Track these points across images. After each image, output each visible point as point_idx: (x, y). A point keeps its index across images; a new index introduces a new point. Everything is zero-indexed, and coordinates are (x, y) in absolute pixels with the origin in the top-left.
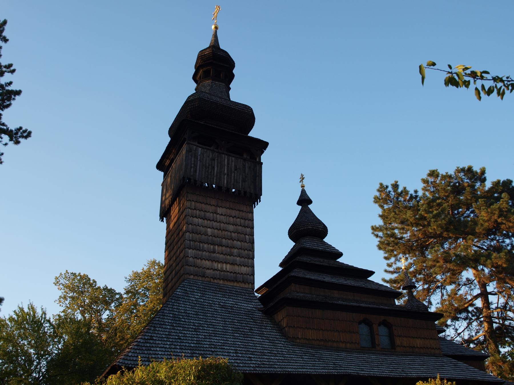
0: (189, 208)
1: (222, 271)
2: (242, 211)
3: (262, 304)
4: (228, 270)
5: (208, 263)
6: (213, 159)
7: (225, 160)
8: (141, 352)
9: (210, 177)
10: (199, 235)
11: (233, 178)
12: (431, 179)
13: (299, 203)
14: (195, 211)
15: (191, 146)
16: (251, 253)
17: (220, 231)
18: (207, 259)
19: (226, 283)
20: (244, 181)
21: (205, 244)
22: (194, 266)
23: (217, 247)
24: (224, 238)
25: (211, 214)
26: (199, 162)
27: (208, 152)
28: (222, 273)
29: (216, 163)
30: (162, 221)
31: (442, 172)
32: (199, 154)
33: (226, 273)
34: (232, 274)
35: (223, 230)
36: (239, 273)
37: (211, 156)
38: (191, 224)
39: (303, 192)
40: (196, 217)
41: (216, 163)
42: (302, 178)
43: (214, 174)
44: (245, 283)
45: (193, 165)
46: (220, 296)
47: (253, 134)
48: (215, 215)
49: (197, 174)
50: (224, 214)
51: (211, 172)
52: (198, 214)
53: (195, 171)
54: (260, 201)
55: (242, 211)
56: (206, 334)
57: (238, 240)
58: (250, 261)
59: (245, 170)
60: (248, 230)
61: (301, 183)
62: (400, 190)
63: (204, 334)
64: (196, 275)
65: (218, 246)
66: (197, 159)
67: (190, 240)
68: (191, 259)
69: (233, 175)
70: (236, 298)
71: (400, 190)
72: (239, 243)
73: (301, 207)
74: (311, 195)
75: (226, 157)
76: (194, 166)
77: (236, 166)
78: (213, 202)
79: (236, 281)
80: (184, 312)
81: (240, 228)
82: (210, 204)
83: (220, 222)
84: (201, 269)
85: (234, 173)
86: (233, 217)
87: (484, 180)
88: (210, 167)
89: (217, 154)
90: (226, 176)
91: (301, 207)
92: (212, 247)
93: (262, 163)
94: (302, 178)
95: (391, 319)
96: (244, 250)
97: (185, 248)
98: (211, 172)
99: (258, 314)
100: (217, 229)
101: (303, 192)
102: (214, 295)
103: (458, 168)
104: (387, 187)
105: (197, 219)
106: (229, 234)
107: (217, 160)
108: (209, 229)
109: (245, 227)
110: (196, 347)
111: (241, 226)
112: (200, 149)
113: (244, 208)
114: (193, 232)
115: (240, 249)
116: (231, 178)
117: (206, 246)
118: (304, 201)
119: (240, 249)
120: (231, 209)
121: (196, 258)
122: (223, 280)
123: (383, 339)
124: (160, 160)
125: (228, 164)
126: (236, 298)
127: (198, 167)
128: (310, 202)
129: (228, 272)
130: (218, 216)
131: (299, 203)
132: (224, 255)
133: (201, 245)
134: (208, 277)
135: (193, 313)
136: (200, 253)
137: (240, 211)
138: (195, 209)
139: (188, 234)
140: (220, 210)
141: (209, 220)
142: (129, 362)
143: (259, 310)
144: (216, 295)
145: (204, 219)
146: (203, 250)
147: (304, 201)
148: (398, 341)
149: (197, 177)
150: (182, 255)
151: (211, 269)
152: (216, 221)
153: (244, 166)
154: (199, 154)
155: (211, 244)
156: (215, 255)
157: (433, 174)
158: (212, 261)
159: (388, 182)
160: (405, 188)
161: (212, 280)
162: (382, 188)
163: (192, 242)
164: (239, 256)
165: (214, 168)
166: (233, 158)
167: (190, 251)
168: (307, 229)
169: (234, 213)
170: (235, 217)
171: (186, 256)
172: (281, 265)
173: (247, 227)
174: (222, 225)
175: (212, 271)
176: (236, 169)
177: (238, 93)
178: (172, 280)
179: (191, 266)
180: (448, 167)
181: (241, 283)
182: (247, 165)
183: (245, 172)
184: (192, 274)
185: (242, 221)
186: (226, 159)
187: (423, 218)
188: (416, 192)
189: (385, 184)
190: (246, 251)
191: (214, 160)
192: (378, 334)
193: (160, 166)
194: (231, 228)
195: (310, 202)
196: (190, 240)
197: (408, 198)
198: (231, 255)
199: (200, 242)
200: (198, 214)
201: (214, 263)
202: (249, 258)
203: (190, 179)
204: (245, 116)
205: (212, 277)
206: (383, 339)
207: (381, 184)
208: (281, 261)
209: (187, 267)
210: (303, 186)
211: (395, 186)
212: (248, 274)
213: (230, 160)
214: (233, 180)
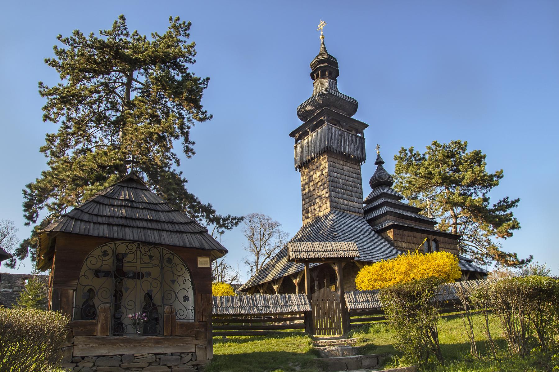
13: (376, 164)
19: (351, 213)
20: (357, 150)
30: (296, 170)
39: (379, 156)
53: (333, 143)
54: (364, 163)
62: (413, 153)
71: (413, 153)
74: (383, 158)
78: (341, 162)
87: (464, 150)
95: (438, 238)
101: (379, 156)
104: (406, 150)
118: (379, 162)
128: (383, 163)
131: (376, 164)
140: (344, 167)
145: (338, 173)
146: (339, 193)
147: (379, 162)
156: (344, 196)
162: (403, 150)
168: (381, 181)
169: (352, 170)
176: (352, 142)
177: (343, 87)
187: (430, 173)
188: (424, 155)
193: (292, 134)
194: (351, 179)
203: (330, 148)
207: (403, 148)
211: (411, 150)
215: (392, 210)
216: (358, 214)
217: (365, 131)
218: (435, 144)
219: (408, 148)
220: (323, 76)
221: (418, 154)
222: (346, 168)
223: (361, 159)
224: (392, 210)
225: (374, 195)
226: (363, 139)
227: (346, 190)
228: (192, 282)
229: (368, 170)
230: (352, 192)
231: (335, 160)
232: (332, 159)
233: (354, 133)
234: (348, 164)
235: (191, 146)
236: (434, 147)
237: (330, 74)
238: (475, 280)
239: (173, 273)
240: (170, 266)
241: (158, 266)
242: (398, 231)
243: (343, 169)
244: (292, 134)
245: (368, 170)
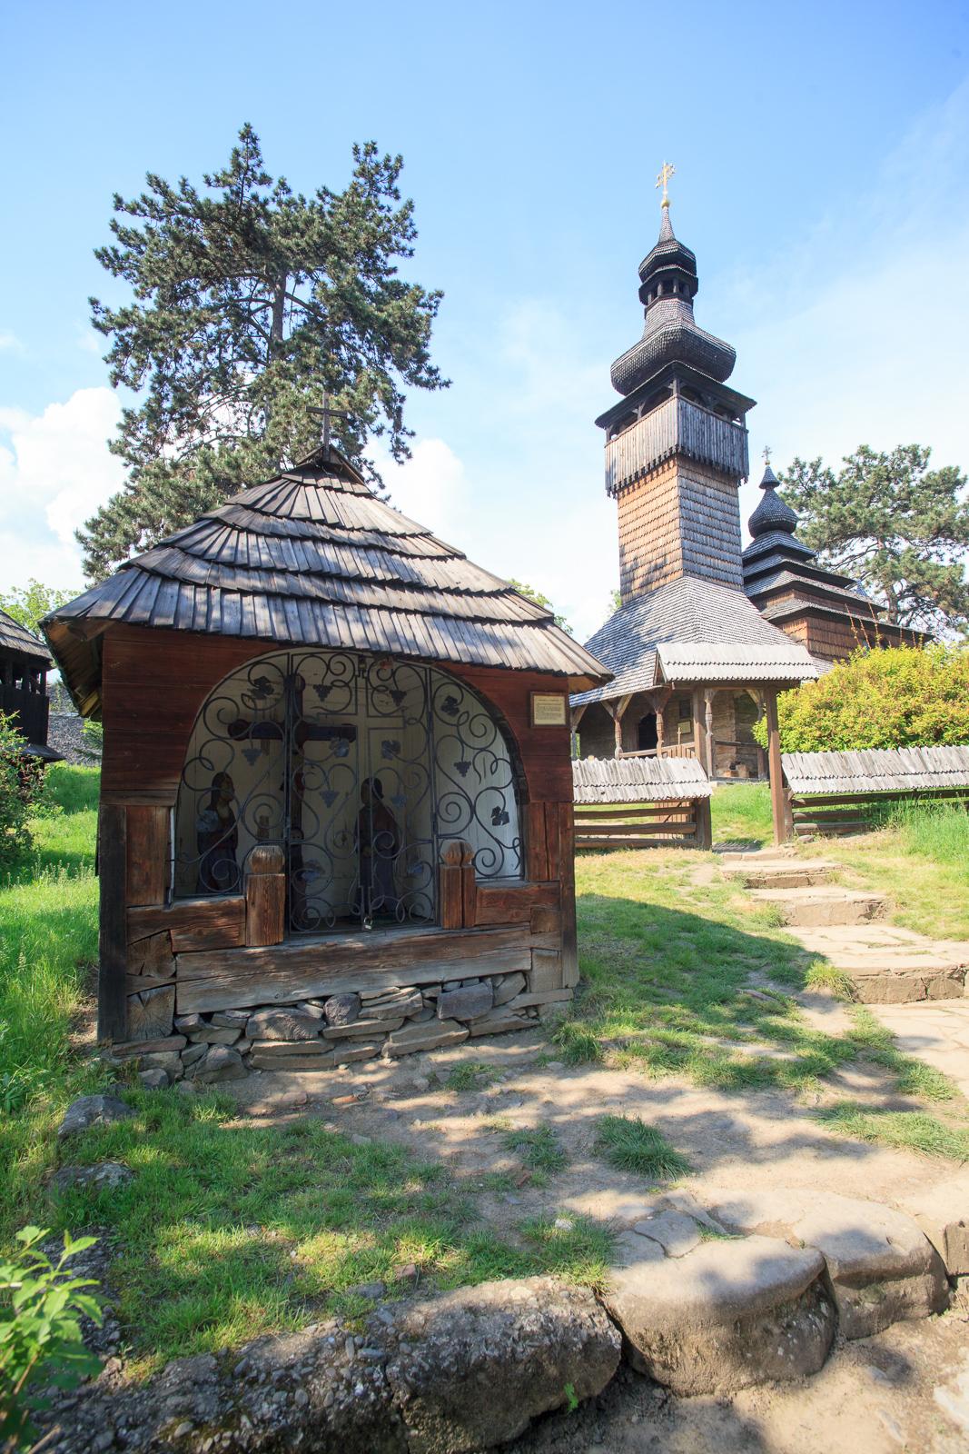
5: (701, 558)
13: (763, 486)
20: (733, 455)
31: (875, 449)
39: (768, 471)
62: (820, 471)
78: (702, 479)
101: (768, 471)
131: (763, 486)
140: (709, 491)
147: (769, 484)
156: (707, 548)
157: (864, 451)
169: (722, 495)
180: (885, 445)
189: (802, 461)
193: (601, 422)
194: (719, 514)
211: (815, 467)
215: (802, 579)
217: (749, 415)
219: (807, 458)
220: (667, 294)
221: (828, 474)
222: (712, 490)
224: (802, 579)
225: (759, 549)
226: (744, 431)
228: (514, 770)
229: (749, 498)
231: (690, 475)
232: (684, 473)
233: (725, 418)
234: (714, 484)
235: (404, 438)
236: (860, 460)
237: (681, 289)
239: (462, 742)
240: (454, 720)
241: (419, 721)
242: (816, 622)
243: (704, 494)
244: (601, 422)
245: (749, 498)
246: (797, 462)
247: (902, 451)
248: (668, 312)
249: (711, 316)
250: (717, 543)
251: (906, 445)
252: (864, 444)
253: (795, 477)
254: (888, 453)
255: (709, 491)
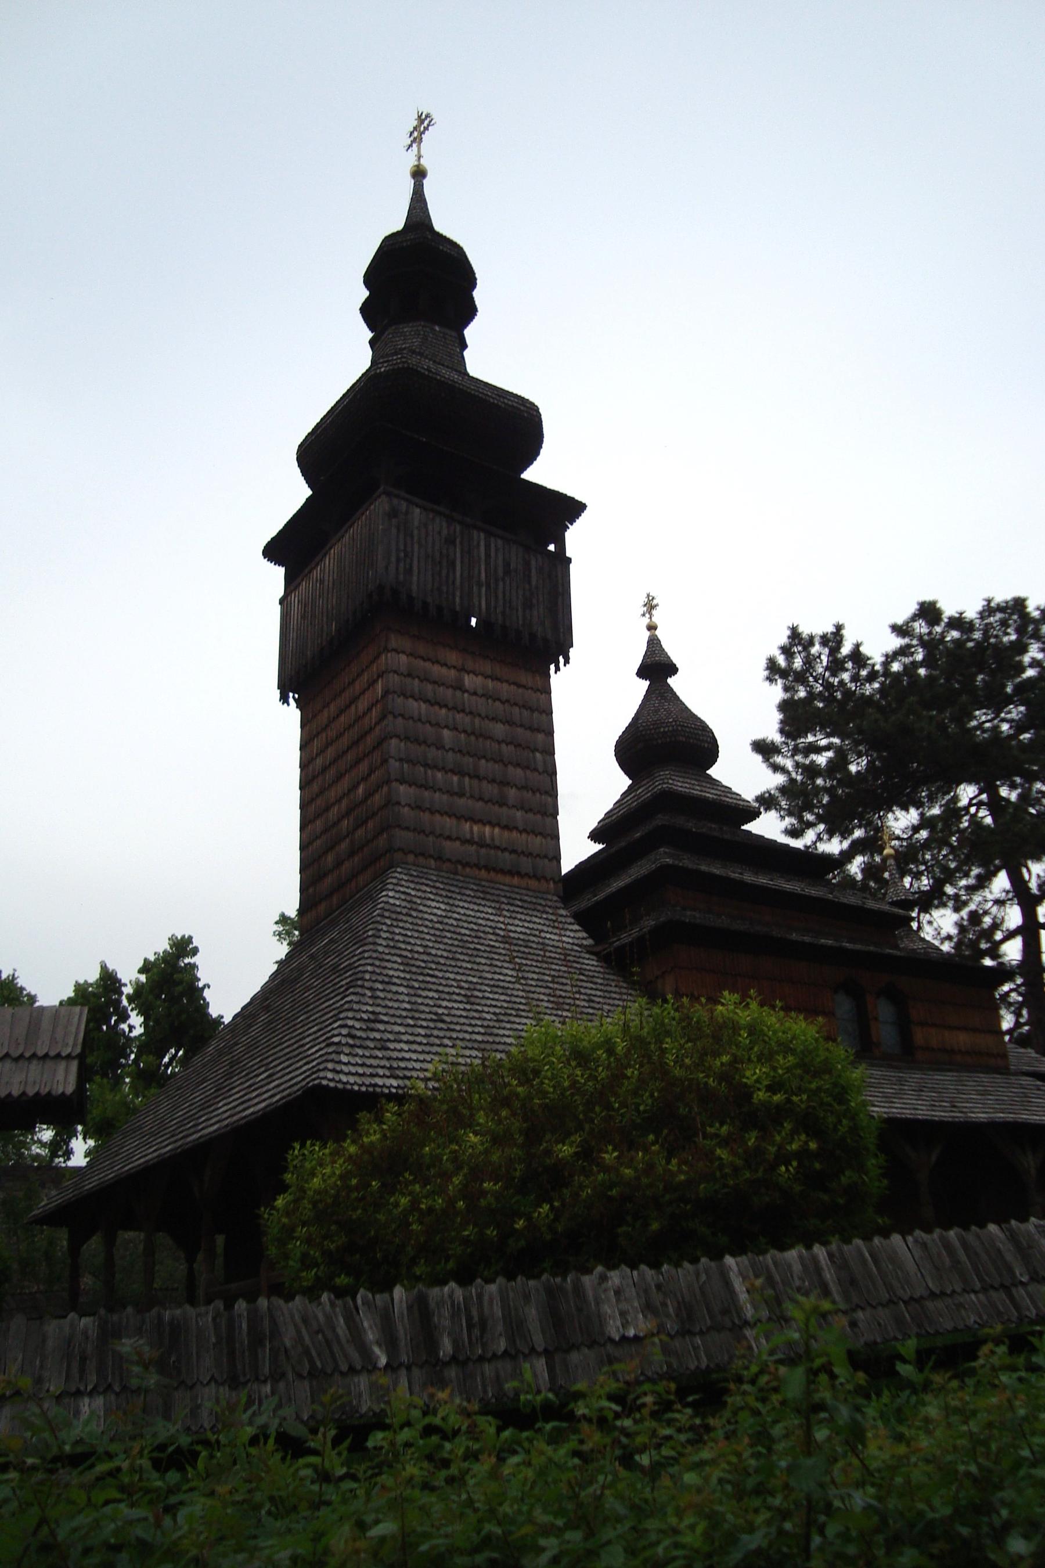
0: (395, 672)
1: (482, 846)
2: (524, 687)
3: (591, 937)
4: (497, 843)
6: (450, 541)
7: (478, 544)
8: (367, 1054)
9: (444, 588)
10: (423, 747)
11: (500, 596)
12: (920, 627)
13: (642, 673)
14: (409, 680)
15: (395, 501)
16: (550, 799)
17: (473, 738)
18: (446, 813)
21: (439, 770)
22: (415, 830)
23: (467, 779)
24: (484, 757)
25: (450, 691)
26: (416, 546)
27: (438, 520)
28: (483, 851)
29: (458, 555)
31: (949, 610)
32: (416, 523)
33: (492, 852)
34: (507, 854)
35: (481, 735)
36: (523, 852)
37: (445, 532)
38: (402, 715)
39: (654, 644)
40: (412, 697)
41: (458, 555)
42: (650, 606)
43: (454, 583)
44: (539, 880)
45: (402, 555)
46: (490, 911)
47: (532, 474)
48: (458, 693)
49: (415, 578)
50: (480, 691)
51: (447, 576)
52: (416, 690)
53: (409, 571)
54: (567, 661)
55: (524, 687)
56: (498, 1011)
57: (518, 765)
58: (548, 820)
59: (529, 577)
60: (540, 737)
61: (646, 620)
62: (846, 650)
63: (492, 1010)
64: (423, 855)
65: (470, 777)
66: (412, 537)
67: (401, 760)
68: (406, 809)
69: (501, 584)
70: (528, 918)
72: (519, 771)
73: (648, 683)
75: (482, 535)
76: (406, 556)
77: (507, 564)
79: (519, 874)
80: (424, 953)
81: (520, 730)
82: (446, 665)
83: (471, 713)
84: (431, 838)
85: (503, 580)
86: (503, 703)
88: (444, 564)
89: (458, 528)
90: (484, 589)
91: (648, 683)
92: (455, 778)
93: (569, 560)
94: (650, 606)
96: (534, 792)
97: (388, 782)
98: (447, 576)
99: (591, 963)
100: (465, 731)
101: (654, 644)
102: (476, 908)
103: (989, 601)
105: (415, 704)
106: (495, 746)
107: (461, 543)
108: (446, 732)
109: (531, 729)
110: (488, 1042)
111: (521, 726)
112: (418, 510)
113: (525, 678)
114: (407, 738)
115: (523, 787)
116: (496, 597)
117: (439, 775)
118: (657, 668)
119: (523, 787)
120: (497, 679)
121: (419, 808)
122: (487, 868)
123: (886, 1034)
124: (280, 532)
125: (488, 555)
126: (528, 918)
127: (415, 562)
128: (672, 669)
129: (497, 848)
130: (466, 695)
131: (642, 673)
132: (486, 802)
133: (429, 772)
134: (449, 860)
135: (445, 954)
136: (426, 794)
137: (519, 686)
138: (409, 675)
139: (394, 742)
140: (469, 681)
141: (446, 706)
142: (352, 1079)
143: (588, 952)
144: (481, 908)
146: (434, 789)
147: (657, 668)
148: (919, 1036)
149: (414, 587)
150: (378, 799)
151: (458, 838)
152: (463, 711)
153: (527, 564)
154: (416, 523)
155: (453, 772)
156: (461, 802)
158: (459, 818)
159: (815, 626)
160: (857, 646)
161: (460, 867)
163: (405, 766)
164: (522, 808)
165: (453, 564)
166: (500, 542)
167: (402, 788)
168: (665, 741)
169: (505, 690)
170: (507, 701)
171: (390, 803)
172: (594, 836)
173: (538, 730)
174: (477, 720)
175: (458, 843)
176: (507, 572)
178: (338, 864)
179: (407, 828)
180: (962, 601)
181: (530, 877)
182: (533, 563)
183: (529, 583)
184: (411, 852)
185: (526, 713)
186: (482, 543)
189: (805, 630)
190: (538, 795)
191: (453, 542)
192: (876, 1019)
193: (273, 551)
194: (499, 729)
195: (672, 669)
196: (401, 760)
197: (864, 673)
198: (502, 803)
199: (426, 765)
200: (416, 690)
201: (463, 821)
202: (544, 814)
204: (518, 426)
205: (459, 862)
206: (886, 1034)
208: (593, 825)
209: (397, 832)
210: (652, 628)
212: (546, 857)
213: (493, 545)
214: (501, 602)
216: (533, 883)
218: (928, 612)
221: (858, 657)
223: (552, 641)
224: (687, 862)
227: (476, 776)
230: (504, 783)
234: (487, 667)
238: (1001, 1220)
243: (459, 687)
244: (273, 551)
246: (795, 634)
247: (989, 609)
248: (409, 336)
249: (493, 353)
250: (490, 790)
251: (1002, 595)
252: (928, 598)
253: (798, 663)
254: (971, 613)
255: (468, 680)
